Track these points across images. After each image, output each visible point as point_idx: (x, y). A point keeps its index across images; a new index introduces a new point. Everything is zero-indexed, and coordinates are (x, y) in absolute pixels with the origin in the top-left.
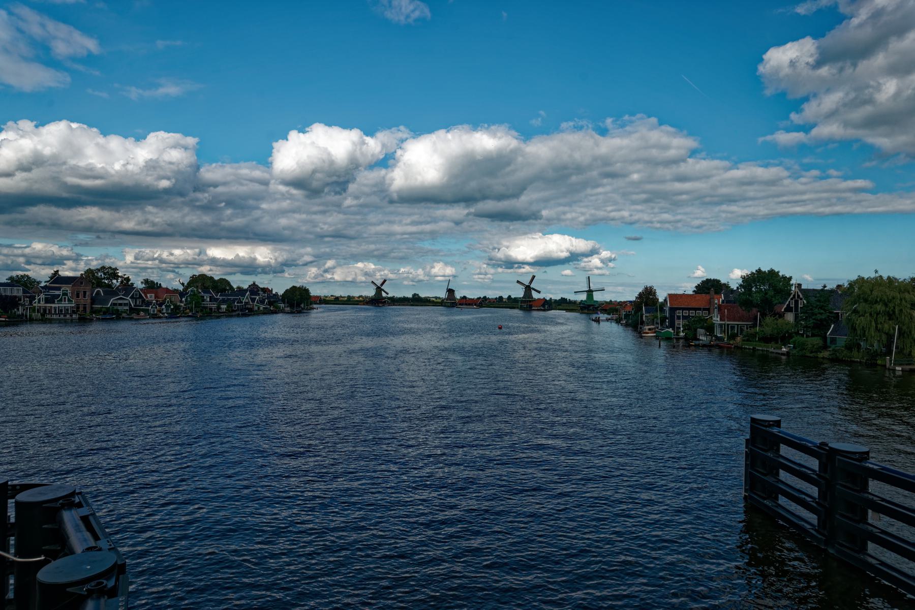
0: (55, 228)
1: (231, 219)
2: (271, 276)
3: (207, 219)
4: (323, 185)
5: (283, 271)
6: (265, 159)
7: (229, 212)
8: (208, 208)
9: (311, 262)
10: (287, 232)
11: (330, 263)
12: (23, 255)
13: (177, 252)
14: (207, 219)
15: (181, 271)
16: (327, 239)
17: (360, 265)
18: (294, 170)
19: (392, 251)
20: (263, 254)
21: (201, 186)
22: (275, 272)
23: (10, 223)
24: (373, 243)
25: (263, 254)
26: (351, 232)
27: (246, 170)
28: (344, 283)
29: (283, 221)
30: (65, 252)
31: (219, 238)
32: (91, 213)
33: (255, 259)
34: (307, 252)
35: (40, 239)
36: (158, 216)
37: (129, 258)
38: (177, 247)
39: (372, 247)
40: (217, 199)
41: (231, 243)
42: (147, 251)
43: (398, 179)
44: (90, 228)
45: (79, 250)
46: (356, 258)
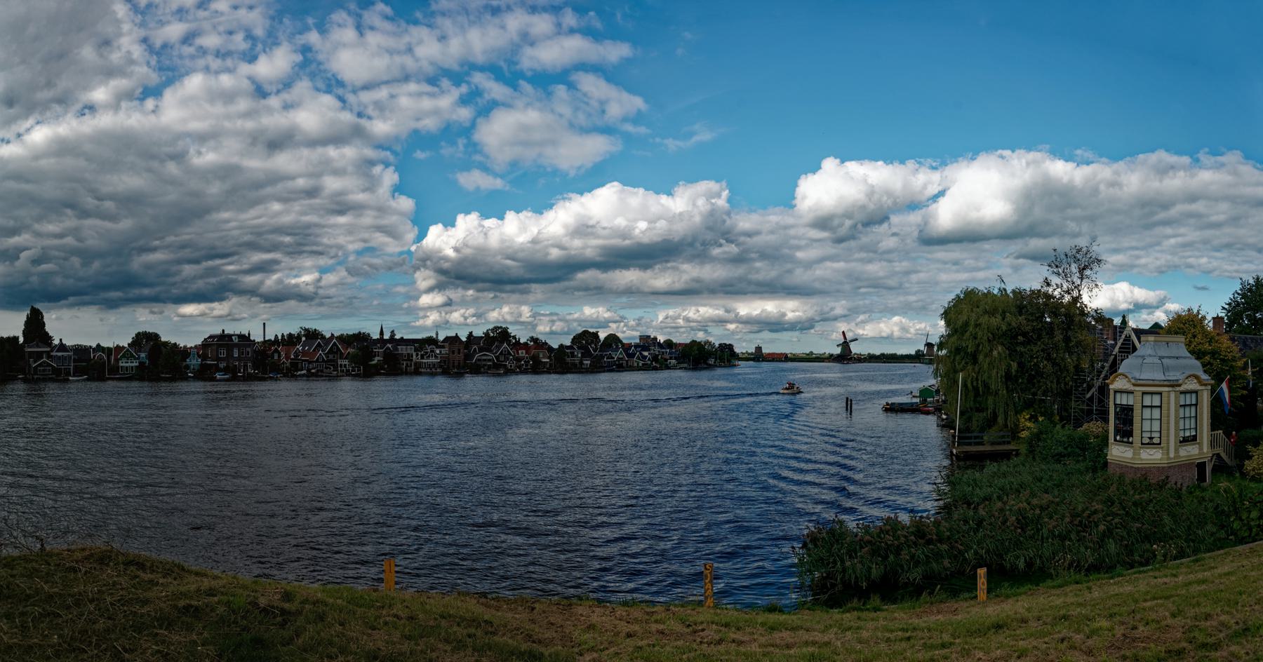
0: (597, 292)
1: (763, 271)
2: (797, 333)
3: (739, 271)
4: (856, 226)
5: (812, 327)
6: (788, 200)
7: (758, 264)
8: (738, 260)
9: (845, 316)
10: (817, 285)
11: (862, 317)
12: (575, 320)
13: (702, 310)
14: (739, 271)
15: (710, 330)
16: (863, 290)
17: (896, 319)
18: (863, 207)
19: (932, 303)
20: (791, 309)
21: (728, 236)
22: (802, 329)
23: (564, 291)
24: (914, 294)
25: (791, 309)
26: (891, 283)
27: (774, 218)
28: (874, 340)
29: (819, 272)
30: (607, 315)
31: (745, 294)
32: (630, 276)
33: (784, 315)
34: (839, 307)
35: (592, 305)
36: (689, 271)
37: (661, 318)
38: (705, 305)
39: (912, 298)
40: (746, 251)
41: (761, 298)
42: (678, 310)
43: (946, 215)
44: (629, 291)
45: (622, 312)
46: (893, 312)
